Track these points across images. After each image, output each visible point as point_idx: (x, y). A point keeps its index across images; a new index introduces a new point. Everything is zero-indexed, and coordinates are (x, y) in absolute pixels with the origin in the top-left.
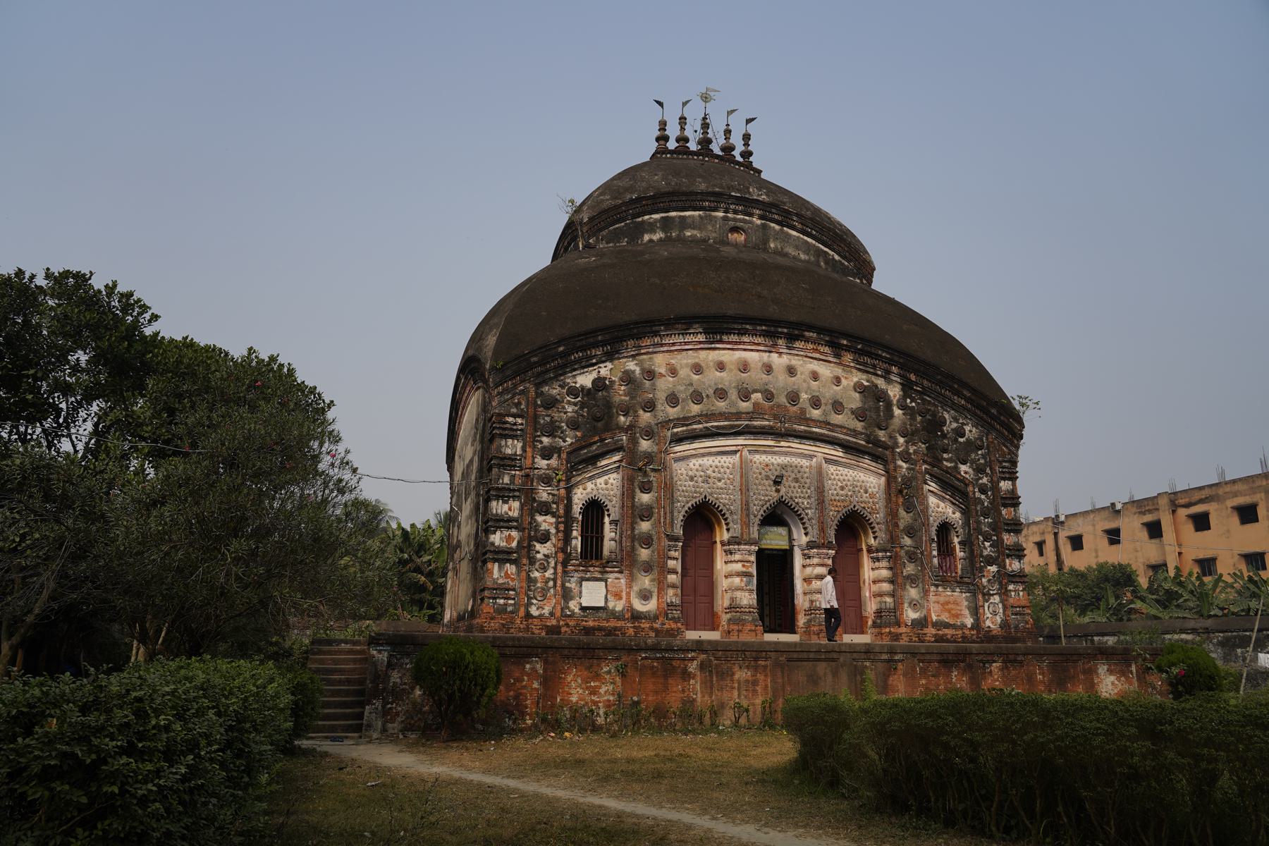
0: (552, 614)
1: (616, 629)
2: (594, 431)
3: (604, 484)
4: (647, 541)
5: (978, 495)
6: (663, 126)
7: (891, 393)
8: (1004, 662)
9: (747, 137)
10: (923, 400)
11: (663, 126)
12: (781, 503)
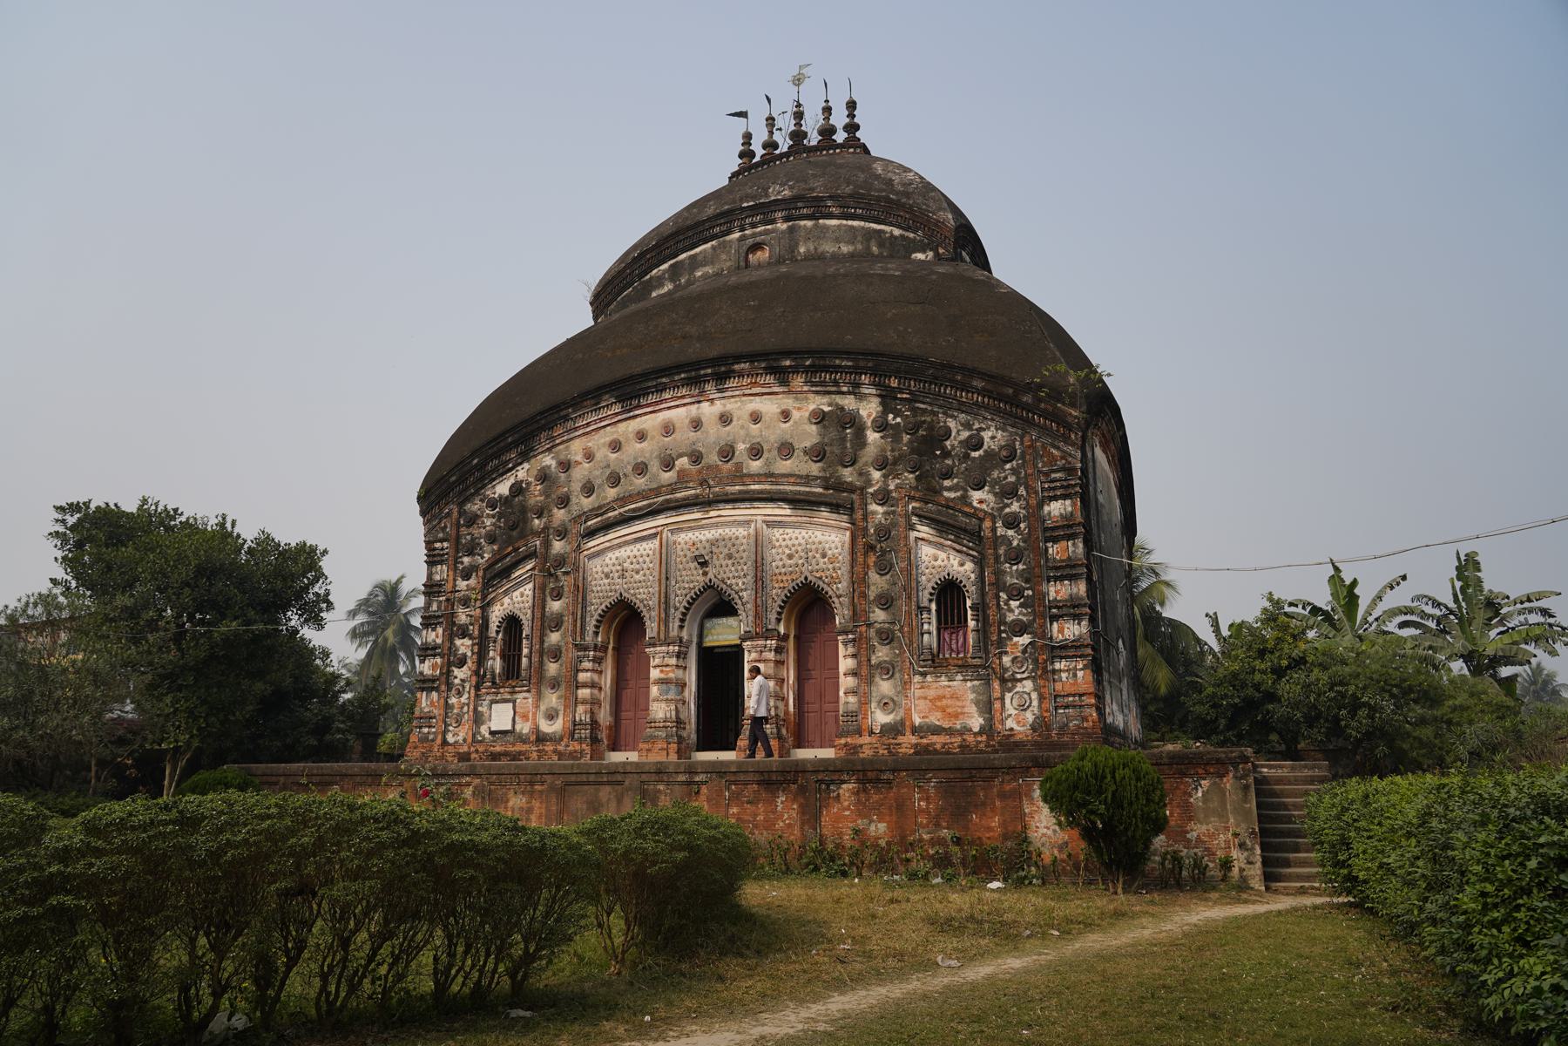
1: (520, 753)
2: (510, 541)
3: (517, 599)
4: (556, 654)
5: (1000, 531)
6: (748, 137)
7: (863, 413)
8: (858, 781)
9: (852, 105)
10: (914, 410)
11: (748, 137)
12: (709, 587)
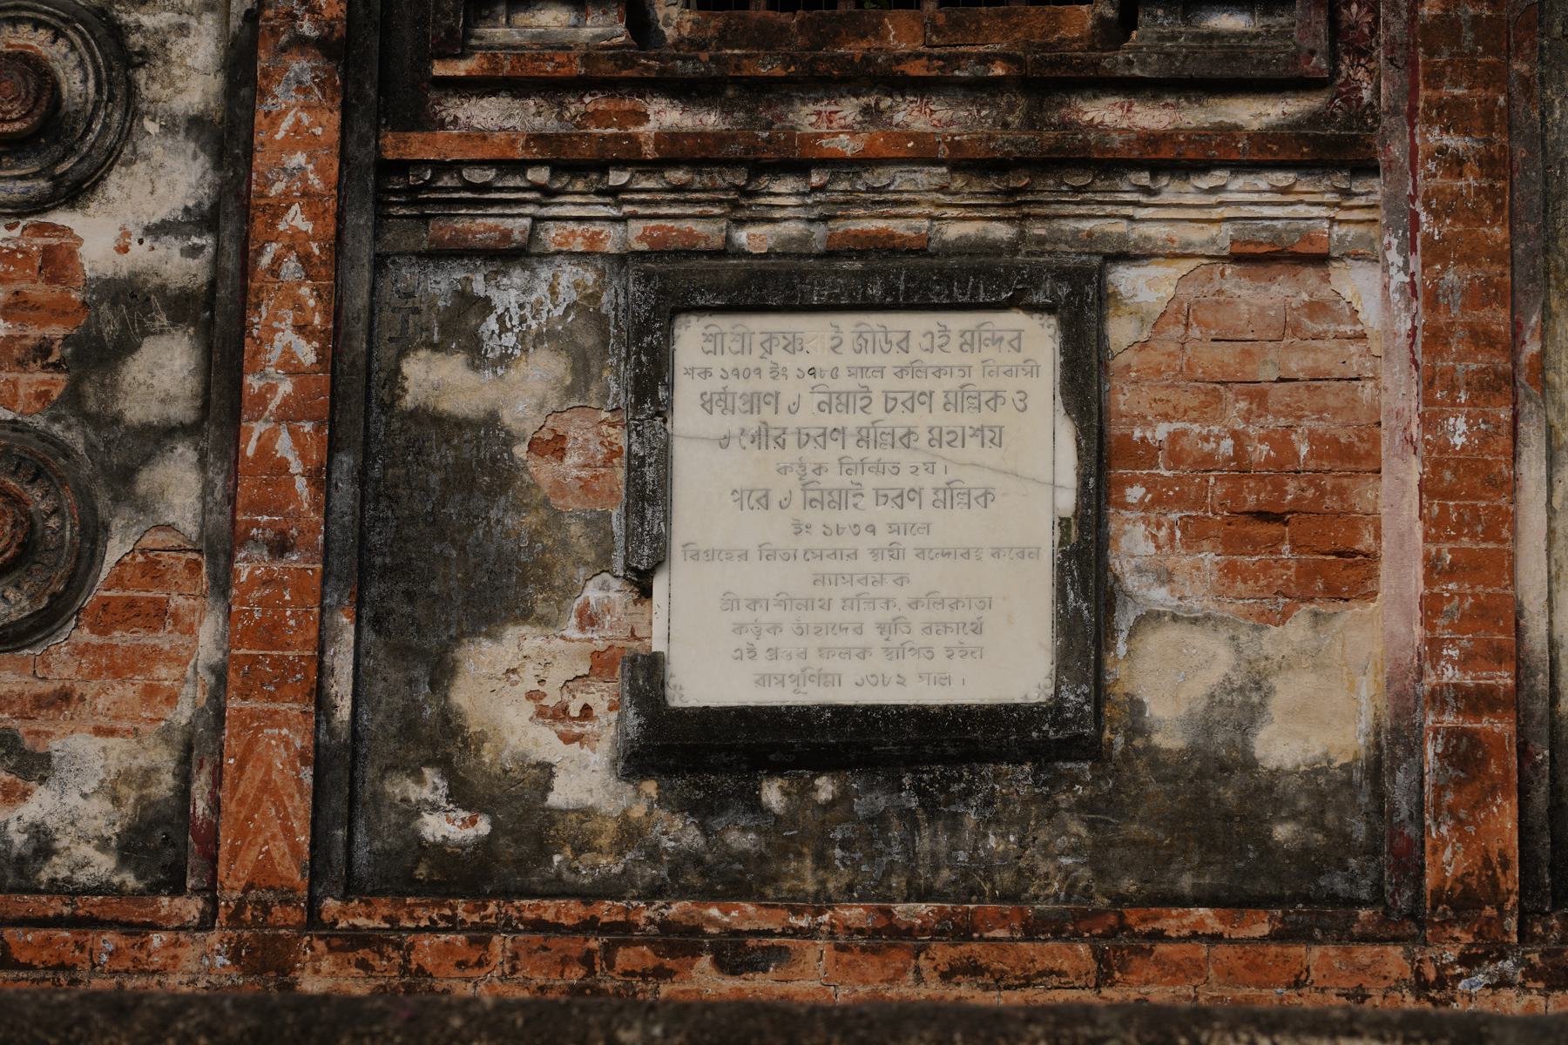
0: (164, 844)
